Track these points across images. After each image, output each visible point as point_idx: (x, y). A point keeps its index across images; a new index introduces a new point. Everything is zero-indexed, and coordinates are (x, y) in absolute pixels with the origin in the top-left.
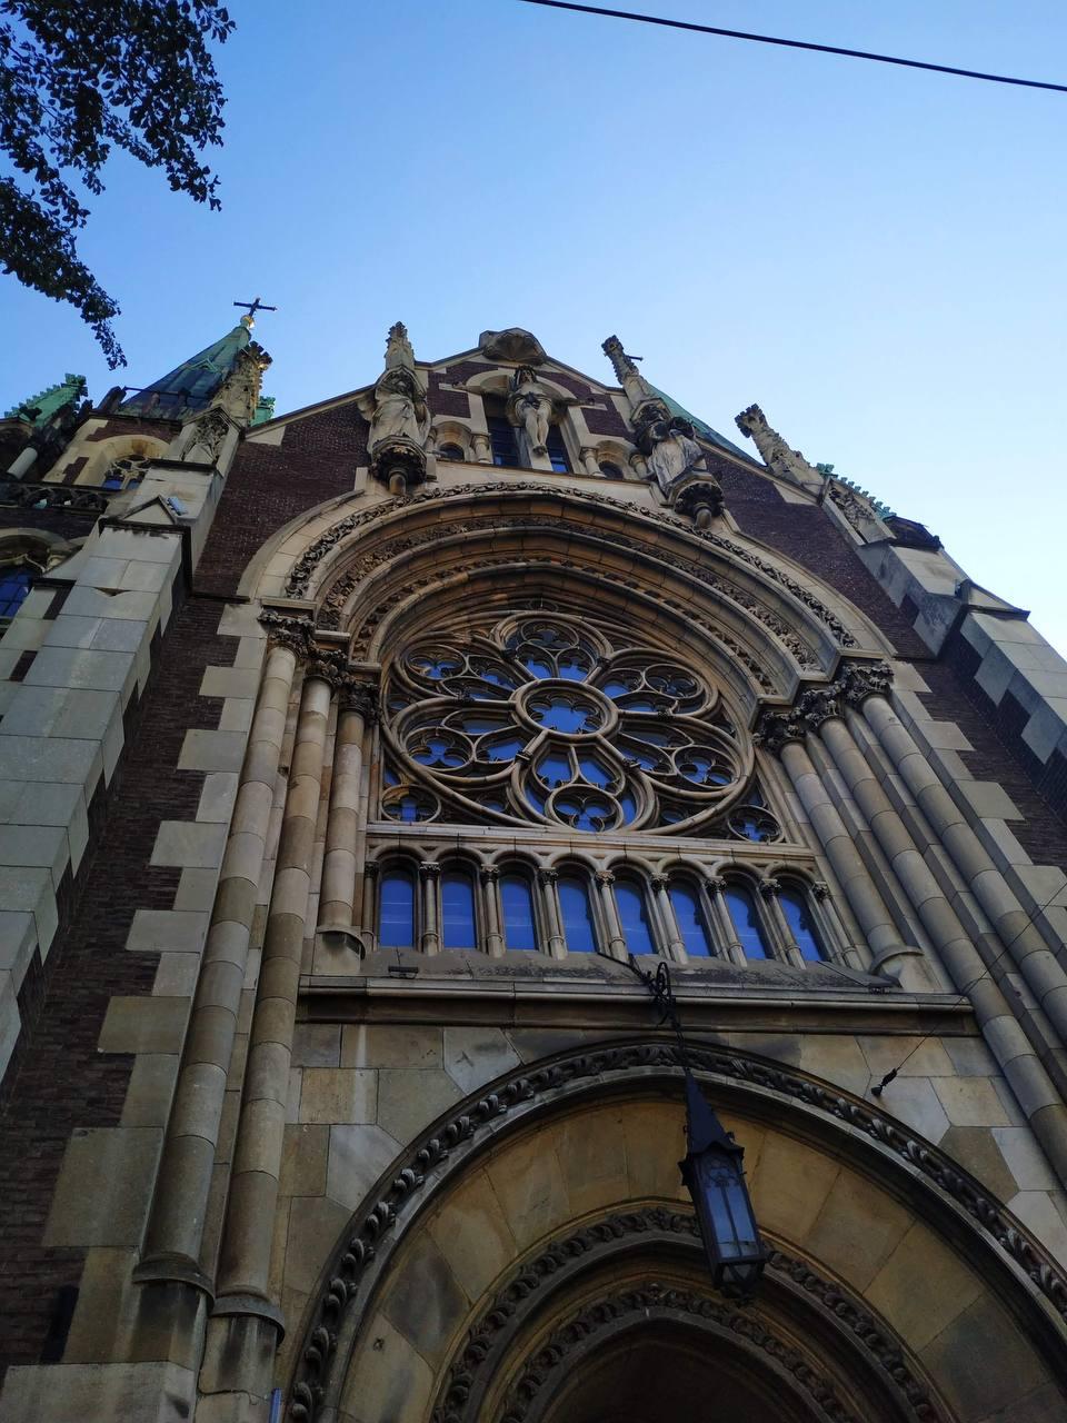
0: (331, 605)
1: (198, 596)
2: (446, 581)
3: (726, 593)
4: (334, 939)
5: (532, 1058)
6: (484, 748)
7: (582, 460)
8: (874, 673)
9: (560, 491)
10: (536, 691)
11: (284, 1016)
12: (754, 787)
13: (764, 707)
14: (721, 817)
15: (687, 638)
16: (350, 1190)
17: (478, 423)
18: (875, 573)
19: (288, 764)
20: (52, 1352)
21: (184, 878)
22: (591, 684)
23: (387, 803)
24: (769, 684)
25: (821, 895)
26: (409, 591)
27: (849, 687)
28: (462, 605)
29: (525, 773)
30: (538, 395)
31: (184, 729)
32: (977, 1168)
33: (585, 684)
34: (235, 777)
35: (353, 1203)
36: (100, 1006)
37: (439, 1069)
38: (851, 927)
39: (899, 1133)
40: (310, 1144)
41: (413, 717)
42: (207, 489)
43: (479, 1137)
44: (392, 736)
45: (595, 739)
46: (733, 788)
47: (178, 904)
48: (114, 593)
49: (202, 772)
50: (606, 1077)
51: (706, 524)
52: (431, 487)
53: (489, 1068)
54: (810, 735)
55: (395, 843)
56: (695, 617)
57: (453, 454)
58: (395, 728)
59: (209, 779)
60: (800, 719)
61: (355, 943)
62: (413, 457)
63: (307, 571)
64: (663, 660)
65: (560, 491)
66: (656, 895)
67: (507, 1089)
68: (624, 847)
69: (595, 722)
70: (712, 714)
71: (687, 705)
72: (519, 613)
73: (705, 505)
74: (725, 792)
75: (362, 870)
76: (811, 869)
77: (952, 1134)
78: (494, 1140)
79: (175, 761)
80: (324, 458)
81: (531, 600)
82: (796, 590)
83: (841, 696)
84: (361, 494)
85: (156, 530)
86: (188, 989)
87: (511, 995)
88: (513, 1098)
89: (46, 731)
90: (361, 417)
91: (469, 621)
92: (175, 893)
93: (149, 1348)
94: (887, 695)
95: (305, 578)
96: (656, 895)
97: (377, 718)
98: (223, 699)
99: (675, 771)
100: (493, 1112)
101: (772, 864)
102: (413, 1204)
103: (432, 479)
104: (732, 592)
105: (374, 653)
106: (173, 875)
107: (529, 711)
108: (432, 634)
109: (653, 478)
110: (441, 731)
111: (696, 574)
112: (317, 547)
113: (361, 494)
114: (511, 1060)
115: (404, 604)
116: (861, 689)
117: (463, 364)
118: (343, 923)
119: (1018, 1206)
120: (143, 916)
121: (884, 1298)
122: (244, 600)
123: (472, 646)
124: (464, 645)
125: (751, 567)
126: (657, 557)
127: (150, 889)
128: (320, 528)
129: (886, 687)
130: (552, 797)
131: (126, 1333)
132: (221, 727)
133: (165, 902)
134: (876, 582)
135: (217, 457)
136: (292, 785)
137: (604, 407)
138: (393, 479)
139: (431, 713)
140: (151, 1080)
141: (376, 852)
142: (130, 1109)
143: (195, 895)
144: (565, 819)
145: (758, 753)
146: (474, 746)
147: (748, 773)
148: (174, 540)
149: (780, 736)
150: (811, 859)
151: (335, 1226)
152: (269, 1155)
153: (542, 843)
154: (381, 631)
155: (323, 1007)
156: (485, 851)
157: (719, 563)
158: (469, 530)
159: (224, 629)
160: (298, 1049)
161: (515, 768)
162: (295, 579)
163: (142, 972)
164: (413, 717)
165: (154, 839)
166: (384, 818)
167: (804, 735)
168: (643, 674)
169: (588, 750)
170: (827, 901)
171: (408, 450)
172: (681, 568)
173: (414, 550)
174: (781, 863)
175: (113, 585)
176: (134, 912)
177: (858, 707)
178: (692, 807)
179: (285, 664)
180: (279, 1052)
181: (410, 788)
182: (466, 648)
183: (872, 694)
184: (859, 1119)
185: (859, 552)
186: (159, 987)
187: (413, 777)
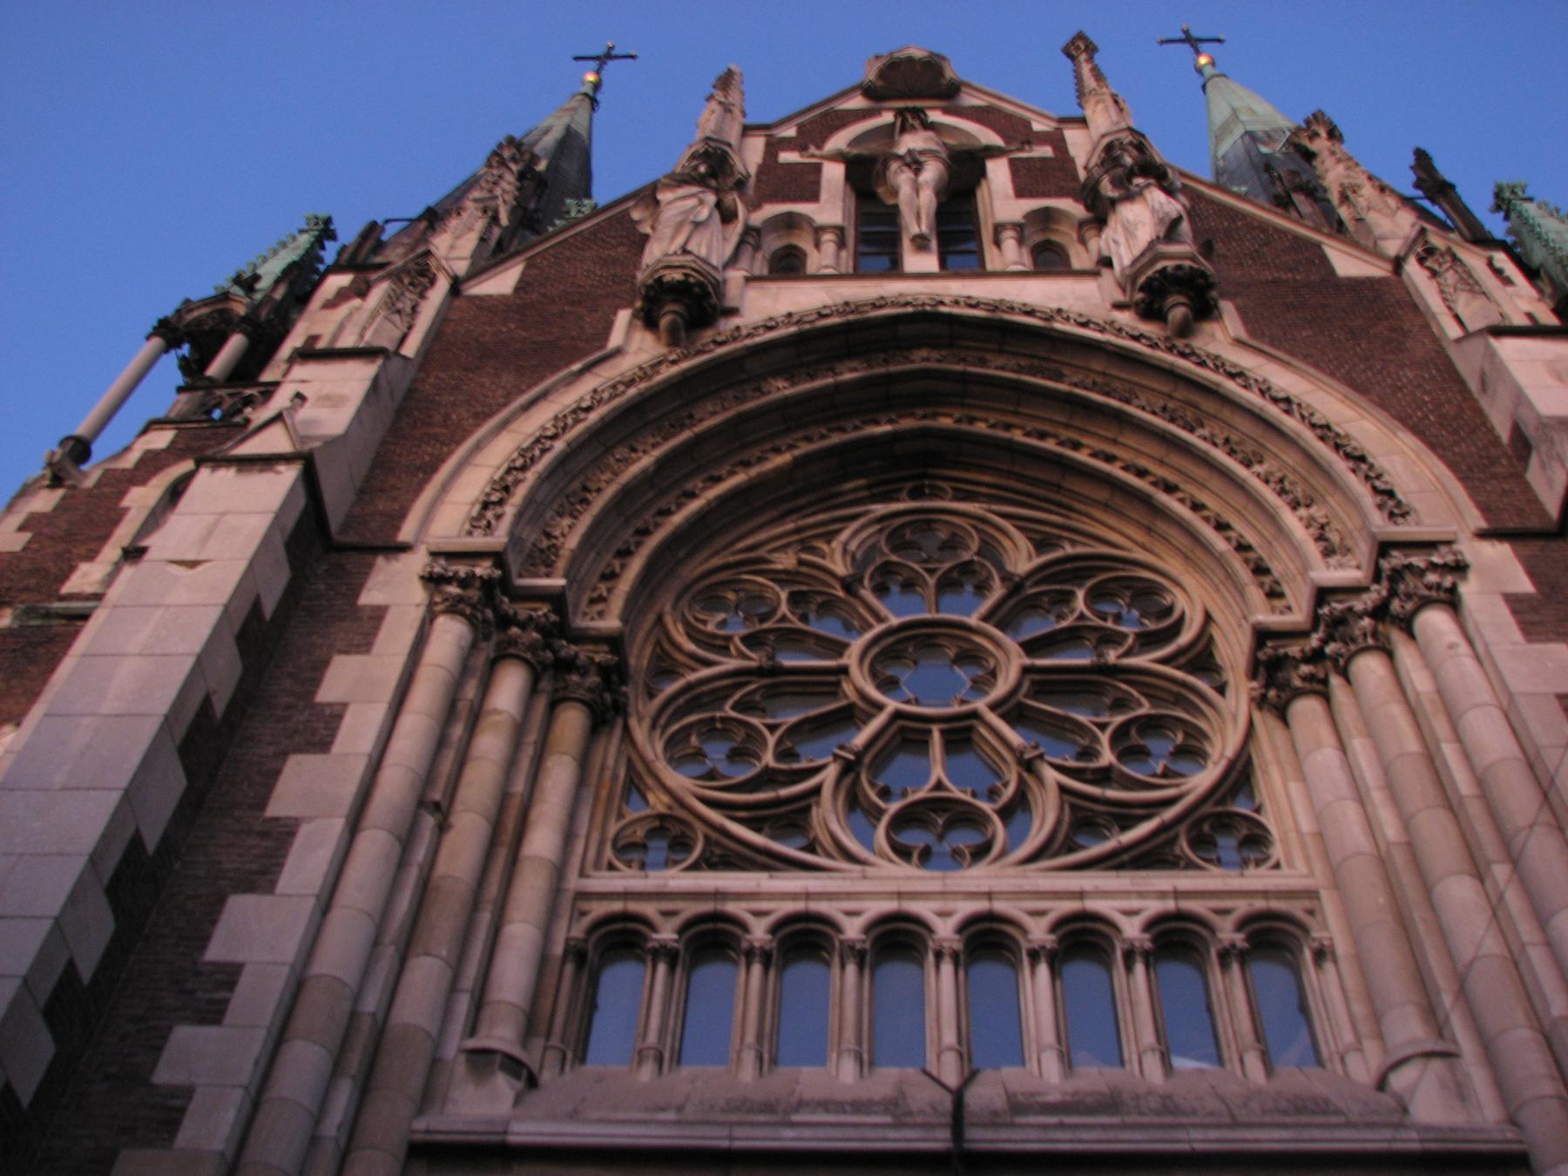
0: (548, 536)
1: (342, 548)
2: (754, 471)
3: (1215, 444)
4: (481, 1060)
6: (789, 744)
7: (997, 243)
8: (1433, 567)
9: (942, 303)
10: (890, 640)
12: (1240, 776)
13: (1262, 635)
14: (1171, 833)
15: (1162, 526)
18: (1473, 385)
19: (437, 795)
21: (245, 980)
22: (986, 619)
23: (621, 843)
24: (1281, 595)
25: (1320, 955)
26: (692, 495)
27: (1393, 593)
28: (791, 505)
29: (847, 781)
30: (922, 153)
31: (283, 755)
33: (973, 620)
34: (338, 825)
38: (1359, 1009)
41: (681, 701)
42: (366, 385)
44: (640, 732)
45: (975, 715)
46: (1201, 780)
47: (229, 1018)
48: (192, 564)
49: (296, 819)
51: (1185, 330)
52: (728, 325)
54: (1335, 681)
55: (617, 906)
56: (1170, 489)
57: (788, 266)
58: (647, 722)
59: (304, 830)
60: (1317, 656)
61: (513, 1065)
62: (692, 285)
63: (506, 489)
64: (1120, 566)
65: (942, 303)
66: (1033, 973)
68: (989, 895)
69: (981, 685)
70: (1189, 655)
71: (1148, 640)
72: (880, 509)
73: (1182, 299)
74: (1183, 789)
75: (558, 949)
76: (1311, 912)
79: (262, 803)
80: (572, 304)
81: (909, 485)
82: (1324, 431)
83: (1380, 612)
84: (618, 352)
85: (267, 462)
87: (725, 1144)
89: (59, 779)
90: (635, 228)
91: (797, 531)
92: (227, 1001)
94: (1452, 602)
95: (501, 502)
96: (1033, 973)
97: (620, 709)
98: (345, 705)
99: (1107, 757)
101: (1242, 907)
103: (733, 312)
104: (1227, 441)
105: (617, 603)
106: (230, 974)
107: (874, 674)
108: (731, 559)
109: (1106, 262)
110: (724, 720)
111: (1167, 416)
112: (531, 448)
113: (618, 352)
115: (678, 519)
116: (1409, 596)
117: (825, 115)
118: (501, 1035)
120: (185, 1036)
122: (405, 548)
123: (798, 573)
124: (785, 572)
125: (1253, 398)
126: (1107, 394)
127: (200, 995)
128: (542, 416)
129: (1453, 590)
130: (885, 820)
132: (337, 748)
133: (213, 1014)
134: (1476, 401)
136: (443, 827)
137: (1046, 151)
138: (664, 322)
139: (713, 691)
141: (586, 921)
144: (903, 853)
145: (1257, 716)
146: (771, 740)
147: (1230, 752)
148: (289, 475)
149: (1284, 686)
150: (1312, 894)
153: (849, 895)
154: (636, 565)
156: (758, 914)
158: (793, 384)
159: (370, 596)
161: (830, 774)
162: (486, 505)
164: (681, 701)
165: (214, 923)
166: (611, 867)
167: (1325, 682)
168: (1080, 594)
169: (961, 734)
170: (1329, 966)
171: (686, 275)
172: (1143, 408)
173: (698, 429)
174: (1260, 904)
175: (191, 557)
176: (170, 1028)
177: (1406, 625)
178: (1125, 816)
179: (450, 634)
181: (661, 817)
182: (783, 578)
183: (1426, 603)
185: (1452, 352)
187: (666, 799)
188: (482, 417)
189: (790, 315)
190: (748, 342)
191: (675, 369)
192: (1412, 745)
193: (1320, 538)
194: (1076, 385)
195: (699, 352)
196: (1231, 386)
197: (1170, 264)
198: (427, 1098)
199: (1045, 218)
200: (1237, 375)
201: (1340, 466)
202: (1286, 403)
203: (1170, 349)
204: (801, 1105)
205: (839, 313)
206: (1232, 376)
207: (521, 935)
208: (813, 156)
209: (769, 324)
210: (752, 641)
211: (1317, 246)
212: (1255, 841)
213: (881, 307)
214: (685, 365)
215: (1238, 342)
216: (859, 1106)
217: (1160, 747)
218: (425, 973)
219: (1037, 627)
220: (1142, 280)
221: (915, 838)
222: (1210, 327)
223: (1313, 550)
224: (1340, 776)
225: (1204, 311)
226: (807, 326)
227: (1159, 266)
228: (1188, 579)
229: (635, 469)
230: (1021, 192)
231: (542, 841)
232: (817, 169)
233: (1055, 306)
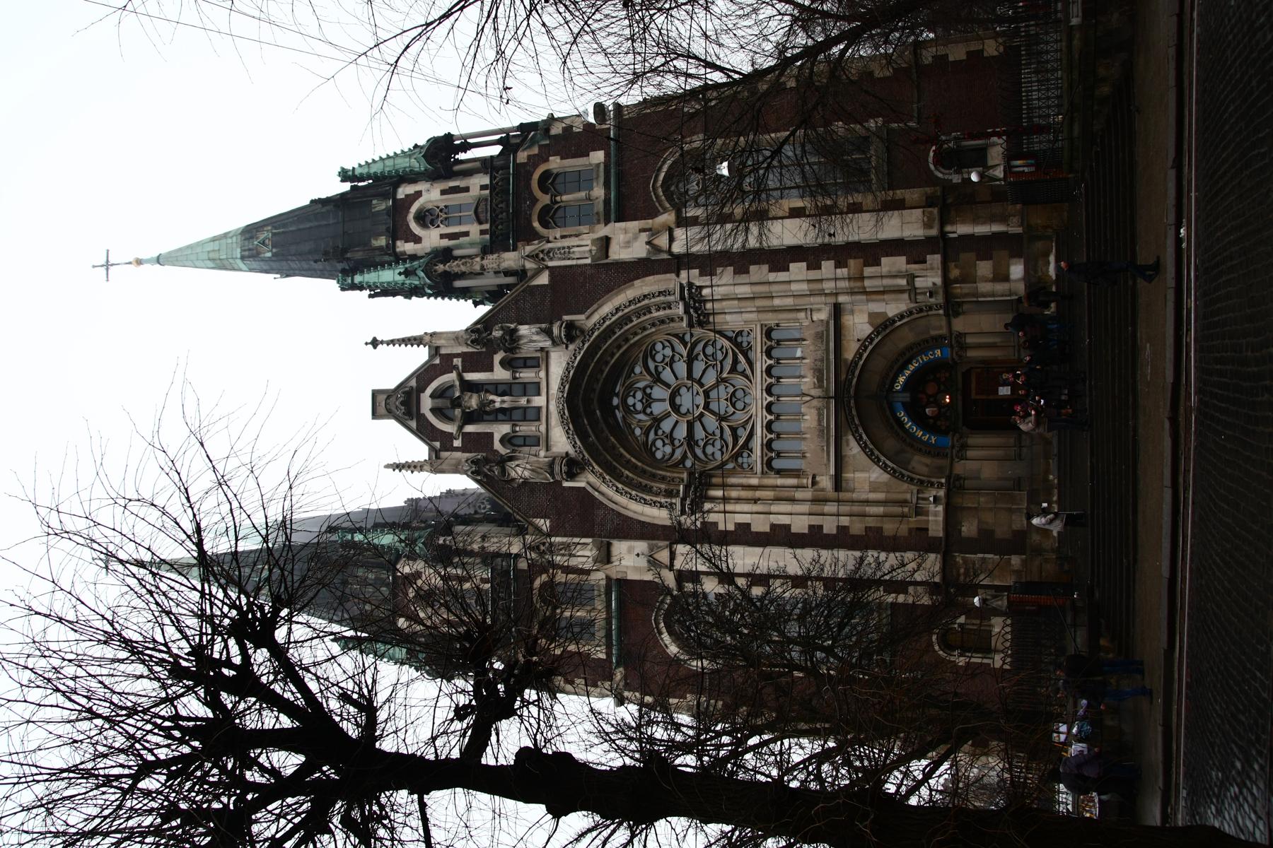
4: (814, 483)
5: (850, 433)
11: (843, 495)
13: (691, 325)
16: (885, 477)
17: (501, 430)
20: (927, 529)
32: (879, 321)
35: (888, 476)
36: (853, 536)
37: (854, 456)
39: (870, 338)
40: (874, 488)
43: (871, 446)
46: (727, 343)
50: (854, 412)
51: (582, 331)
53: (853, 443)
60: (699, 316)
67: (859, 440)
72: (619, 415)
77: (871, 323)
78: (872, 443)
83: (695, 302)
86: (848, 518)
88: (861, 437)
93: (927, 513)
94: (701, 288)
100: (865, 443)
101: (764, 339)
102: (888, 462)
103: (567, 453)
106: (811, 527)
114: (851, 437)
115: (639, 464)
118: (807, 481)
119: (890, 315)
120: (825, 531)
121: (902, 345)
131: (924, 518)
133: (821, 527)
136: (759, 499)
137: (458, 362)
140: (871, 522)
142: (879, 525)
143: (816, 520)
151: (894, 480)
152: (880, 496)
155: (838, 483)
157: (610, 331)
160: (848, 491)
161: (724, 424)
163: (842, 529)
180: (855, 496)
183: (700, 293)
184: (866, 348)
186: (847, 524)
188: (619, 514)
191: (596, 467)
192: (736, 302)
193: (664, 309)
196: (608, 323)
198: (823, 490)
199: (502, 363)
200: (604, 319)
201: (646, 302)
202: (617, 310)
203: (590, 337)
204: (820, 425)
206: (604, 322)
207: (780, 481)
210: (672, 443)
212: (740, 333)
215: (588, 318)
216: (820, 415)
217: (709, 350)
218: (799, 495)
219: (667, 375)
220: (565, 341)
221: (740, 405)
222: (577, 324)
223: (668, 311)
224: (734, 316)
225: (571, 326)
228: (654, 338)
229: (630, 475)
230: (491, 369)
231: (754, 481)
232: (467, 436)
233: (564, 364)
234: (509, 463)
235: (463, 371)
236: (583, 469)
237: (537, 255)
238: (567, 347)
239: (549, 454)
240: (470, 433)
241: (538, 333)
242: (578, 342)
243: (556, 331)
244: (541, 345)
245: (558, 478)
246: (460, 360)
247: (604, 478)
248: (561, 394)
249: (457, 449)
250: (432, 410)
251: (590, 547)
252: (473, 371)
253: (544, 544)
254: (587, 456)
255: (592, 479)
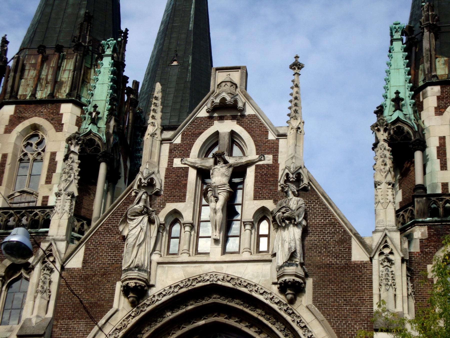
51: (292, 302)
65: (219, 280)
84: (117, 311)
103: (153, 286)
113: (117, 311)
135: (50, 297)
137: (268, 159)
171: (136, 283)
189: (171, 287)
190: (157, 303)
194: (259, 314)
195: (142, 311)
197: (287, 278)
205: (187, 286)
208: (185, 164)
209: (164, 293)
211: (350, 238)
213: (200, 282)
214: (137, 318)
220: (280, 280)
226: (176, 294)
227: (283, 279)
230: (256, 197)
232: (186, 171)
233: (255, 281)
234: (146, 219)
235: (257, 166)
236: (134, 304)
237: (386, 246)
238: (274, 284)
239: (154, 265)
240: (187, 176)
241: (289, 249)
242: (281, 298)
243: (291, 270)
244: (279, 254)
245: (123, 276)
246: (271, 162)
247: (121, 329)
248: (221, 277)
249: (171, 162)
250: (217, 134)
251: (42, 314)
252: (256, 177)
253: (54, 262)
254: (148, 309)
255: (120, 316)
